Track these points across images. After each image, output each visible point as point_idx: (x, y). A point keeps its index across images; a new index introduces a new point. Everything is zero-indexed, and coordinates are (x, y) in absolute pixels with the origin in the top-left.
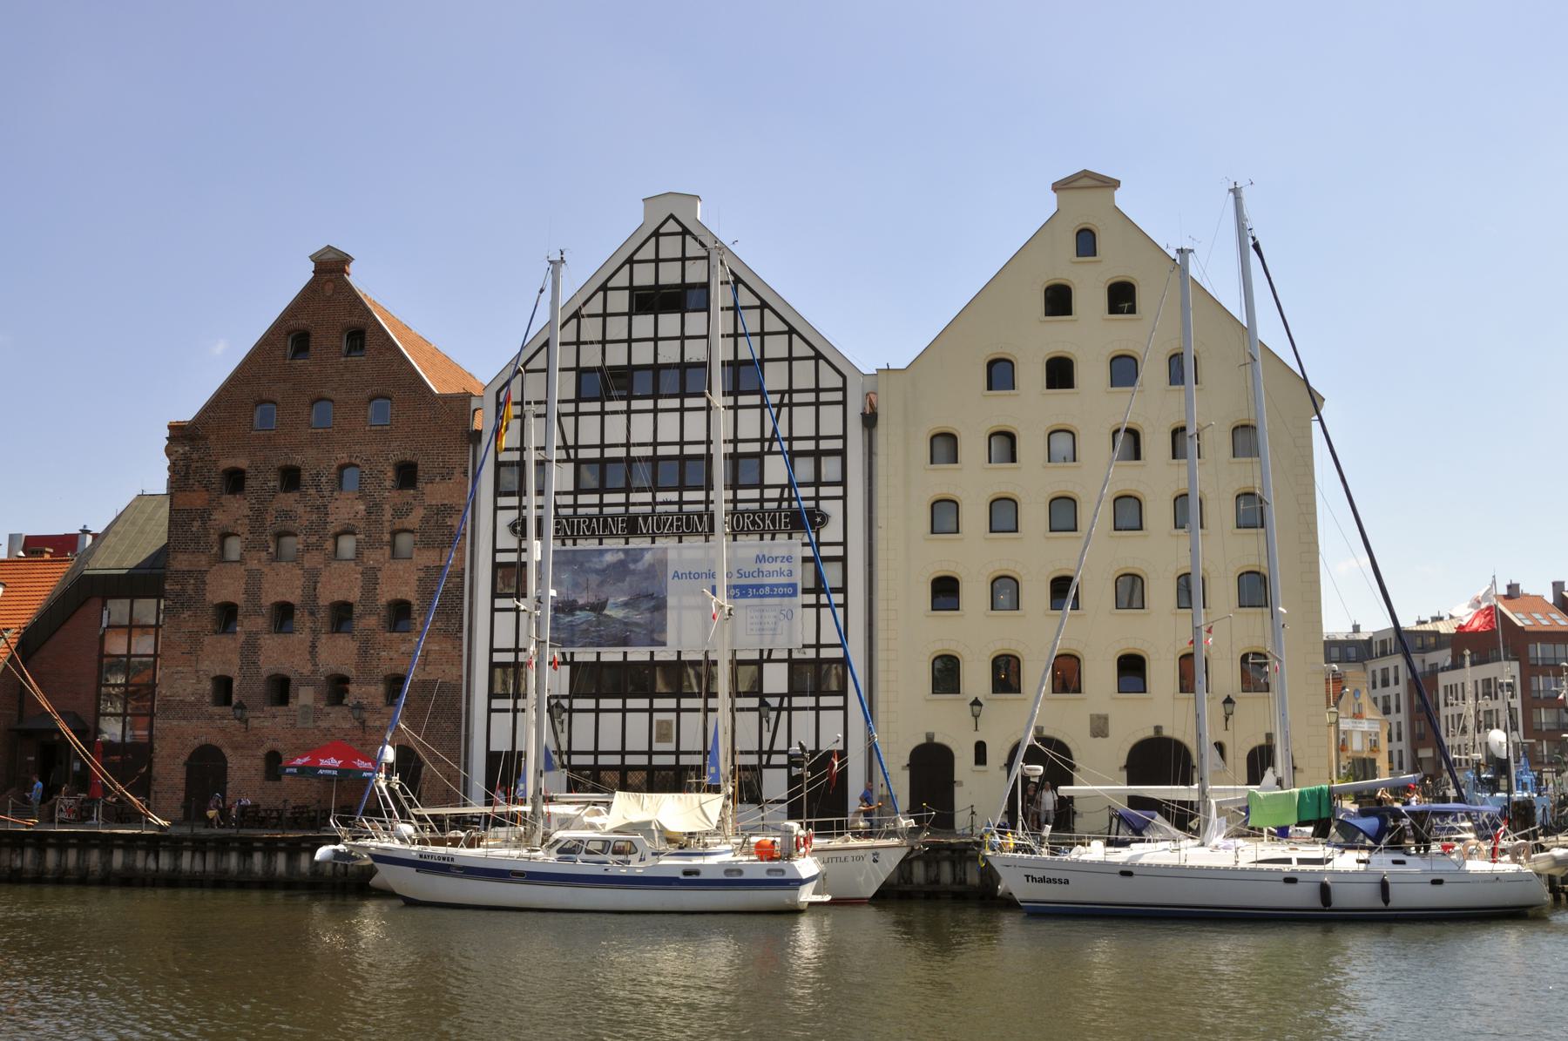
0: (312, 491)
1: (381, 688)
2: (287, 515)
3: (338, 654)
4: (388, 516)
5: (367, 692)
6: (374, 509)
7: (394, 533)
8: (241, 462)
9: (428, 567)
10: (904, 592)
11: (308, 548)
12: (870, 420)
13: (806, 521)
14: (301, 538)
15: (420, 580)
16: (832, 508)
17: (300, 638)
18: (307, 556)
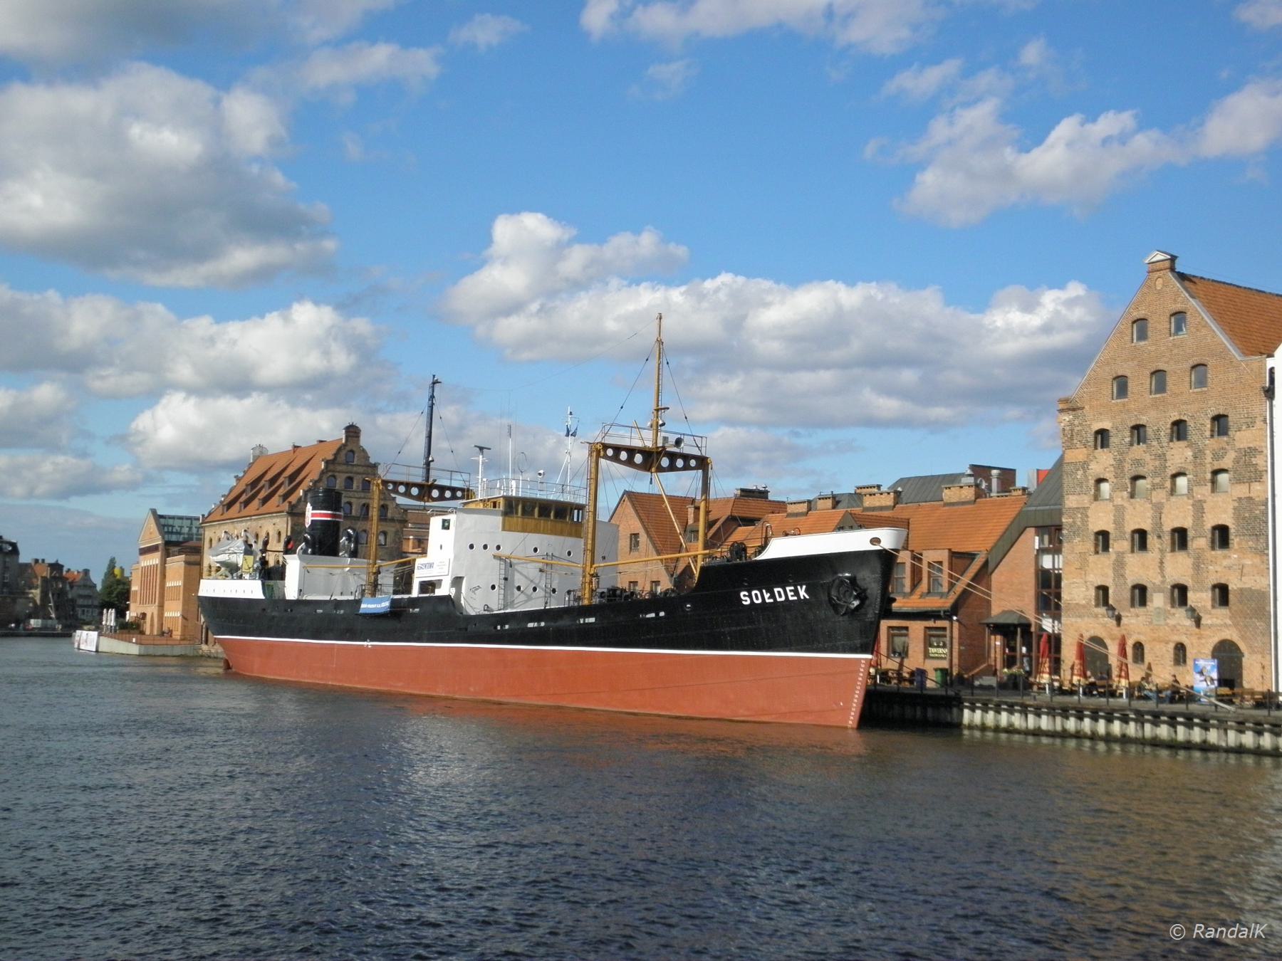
0: (1155, 443)
1: (1210, 594)
2: (1138, 462)
3: (1179, 567)
4: (1209, 459)
5: (1200, 598)
6: (1198, 455)
7: (1216, 473)
8: (1106, 425)
9: (1240, 499)
11: (1154, 487)
14: (1149, 480)
15: (1235, 509)
17: (1152, 555)
18: (1154, 493)
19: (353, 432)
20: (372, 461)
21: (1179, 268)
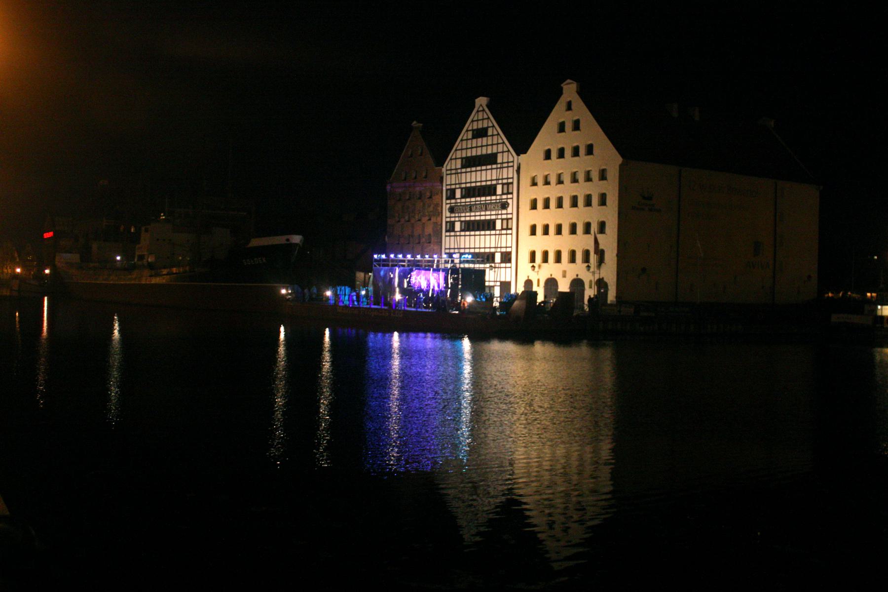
10: (525, 230)
13: (504, 206)
16: (510, 201)
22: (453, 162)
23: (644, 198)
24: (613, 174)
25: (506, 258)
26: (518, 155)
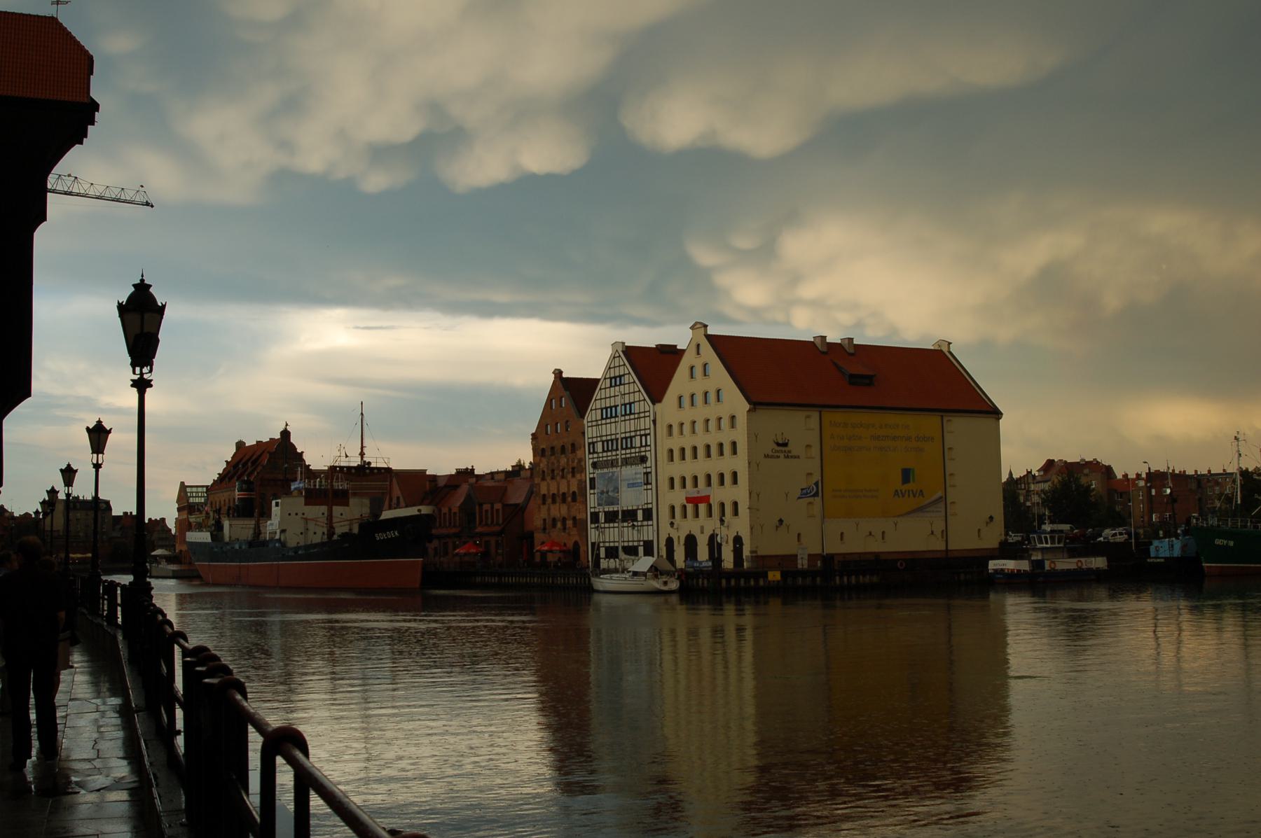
3: (564, 510)
5: (569, 523)
10: (664, 485)
12: (654, 422)
13: (643, 460)
16: (648, 454)
19: (286, 434)
20: (299, 451)
21: (564, 375)
22: (592, 415)
23: (778, 444)
24: (742, 420)
25: (648, 514)
26: (654, 404)
